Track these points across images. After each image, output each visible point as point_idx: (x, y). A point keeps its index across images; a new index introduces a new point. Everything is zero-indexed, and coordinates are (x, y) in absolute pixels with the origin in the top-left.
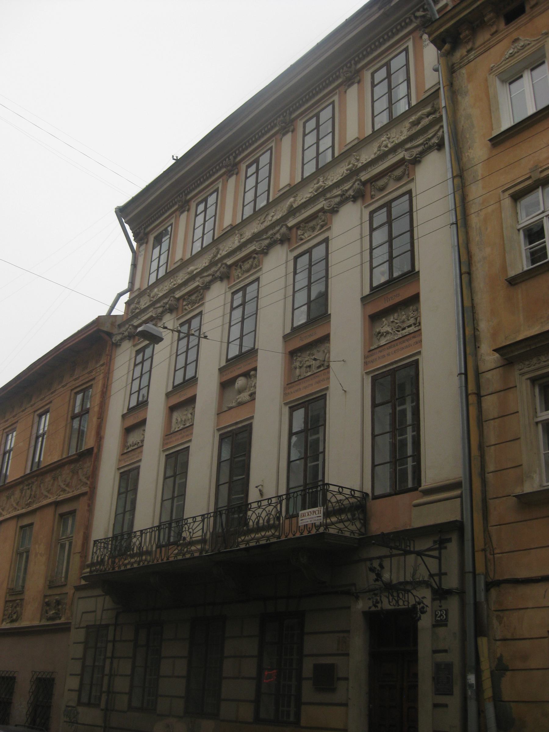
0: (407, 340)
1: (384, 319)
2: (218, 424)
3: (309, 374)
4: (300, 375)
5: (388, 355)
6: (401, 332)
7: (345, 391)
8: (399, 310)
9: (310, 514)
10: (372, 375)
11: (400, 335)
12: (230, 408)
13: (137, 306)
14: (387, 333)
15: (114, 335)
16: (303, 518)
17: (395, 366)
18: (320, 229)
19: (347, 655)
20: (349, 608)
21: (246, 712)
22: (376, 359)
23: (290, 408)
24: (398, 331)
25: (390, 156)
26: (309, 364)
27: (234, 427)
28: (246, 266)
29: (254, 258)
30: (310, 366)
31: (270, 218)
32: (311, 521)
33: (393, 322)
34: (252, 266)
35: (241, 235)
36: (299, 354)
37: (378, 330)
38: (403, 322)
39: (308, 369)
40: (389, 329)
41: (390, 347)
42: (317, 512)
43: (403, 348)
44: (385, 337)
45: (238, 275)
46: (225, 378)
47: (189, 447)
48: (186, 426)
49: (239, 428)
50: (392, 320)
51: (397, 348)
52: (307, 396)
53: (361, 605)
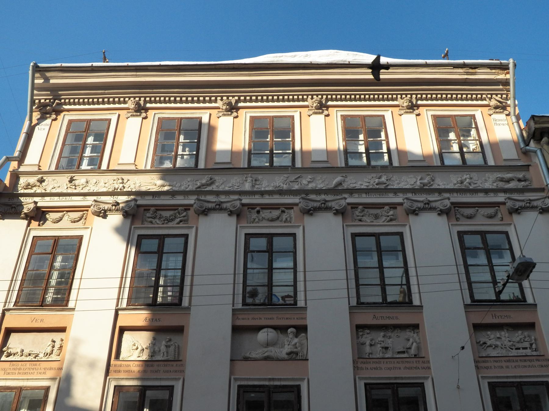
0: (530, 361)
1: (489, 333)
2: (232, 373)
3: (387, 356)
4: (371, 354)
7: (458, 387)
8: (505, 330)
11: (514, 353)
12: (246, 359)
14: (496, 346)
17: (519, 380)
18: (388, 222)
23: (366, 384)
24: (512, 349)
26: (386, 346)
27: (267, 383)
28: (266, 214)
29: (283, 212)
30: (386, 348)
31: (305, 182)
33: (498, 338)
34: (278, 218)
35: (256, 180)
36: (368, 331)
37: (483, 340)
38: (518, 342)
39: (384, 350)
40: (498, 343)
41: (509, 361)
43: (525, 366)
44: (494, 349)
45: (255, 219)
46: (239, 323)
47: (173, 387)
49: (276, 386)
50: (498, 336)
52: (396, 378)
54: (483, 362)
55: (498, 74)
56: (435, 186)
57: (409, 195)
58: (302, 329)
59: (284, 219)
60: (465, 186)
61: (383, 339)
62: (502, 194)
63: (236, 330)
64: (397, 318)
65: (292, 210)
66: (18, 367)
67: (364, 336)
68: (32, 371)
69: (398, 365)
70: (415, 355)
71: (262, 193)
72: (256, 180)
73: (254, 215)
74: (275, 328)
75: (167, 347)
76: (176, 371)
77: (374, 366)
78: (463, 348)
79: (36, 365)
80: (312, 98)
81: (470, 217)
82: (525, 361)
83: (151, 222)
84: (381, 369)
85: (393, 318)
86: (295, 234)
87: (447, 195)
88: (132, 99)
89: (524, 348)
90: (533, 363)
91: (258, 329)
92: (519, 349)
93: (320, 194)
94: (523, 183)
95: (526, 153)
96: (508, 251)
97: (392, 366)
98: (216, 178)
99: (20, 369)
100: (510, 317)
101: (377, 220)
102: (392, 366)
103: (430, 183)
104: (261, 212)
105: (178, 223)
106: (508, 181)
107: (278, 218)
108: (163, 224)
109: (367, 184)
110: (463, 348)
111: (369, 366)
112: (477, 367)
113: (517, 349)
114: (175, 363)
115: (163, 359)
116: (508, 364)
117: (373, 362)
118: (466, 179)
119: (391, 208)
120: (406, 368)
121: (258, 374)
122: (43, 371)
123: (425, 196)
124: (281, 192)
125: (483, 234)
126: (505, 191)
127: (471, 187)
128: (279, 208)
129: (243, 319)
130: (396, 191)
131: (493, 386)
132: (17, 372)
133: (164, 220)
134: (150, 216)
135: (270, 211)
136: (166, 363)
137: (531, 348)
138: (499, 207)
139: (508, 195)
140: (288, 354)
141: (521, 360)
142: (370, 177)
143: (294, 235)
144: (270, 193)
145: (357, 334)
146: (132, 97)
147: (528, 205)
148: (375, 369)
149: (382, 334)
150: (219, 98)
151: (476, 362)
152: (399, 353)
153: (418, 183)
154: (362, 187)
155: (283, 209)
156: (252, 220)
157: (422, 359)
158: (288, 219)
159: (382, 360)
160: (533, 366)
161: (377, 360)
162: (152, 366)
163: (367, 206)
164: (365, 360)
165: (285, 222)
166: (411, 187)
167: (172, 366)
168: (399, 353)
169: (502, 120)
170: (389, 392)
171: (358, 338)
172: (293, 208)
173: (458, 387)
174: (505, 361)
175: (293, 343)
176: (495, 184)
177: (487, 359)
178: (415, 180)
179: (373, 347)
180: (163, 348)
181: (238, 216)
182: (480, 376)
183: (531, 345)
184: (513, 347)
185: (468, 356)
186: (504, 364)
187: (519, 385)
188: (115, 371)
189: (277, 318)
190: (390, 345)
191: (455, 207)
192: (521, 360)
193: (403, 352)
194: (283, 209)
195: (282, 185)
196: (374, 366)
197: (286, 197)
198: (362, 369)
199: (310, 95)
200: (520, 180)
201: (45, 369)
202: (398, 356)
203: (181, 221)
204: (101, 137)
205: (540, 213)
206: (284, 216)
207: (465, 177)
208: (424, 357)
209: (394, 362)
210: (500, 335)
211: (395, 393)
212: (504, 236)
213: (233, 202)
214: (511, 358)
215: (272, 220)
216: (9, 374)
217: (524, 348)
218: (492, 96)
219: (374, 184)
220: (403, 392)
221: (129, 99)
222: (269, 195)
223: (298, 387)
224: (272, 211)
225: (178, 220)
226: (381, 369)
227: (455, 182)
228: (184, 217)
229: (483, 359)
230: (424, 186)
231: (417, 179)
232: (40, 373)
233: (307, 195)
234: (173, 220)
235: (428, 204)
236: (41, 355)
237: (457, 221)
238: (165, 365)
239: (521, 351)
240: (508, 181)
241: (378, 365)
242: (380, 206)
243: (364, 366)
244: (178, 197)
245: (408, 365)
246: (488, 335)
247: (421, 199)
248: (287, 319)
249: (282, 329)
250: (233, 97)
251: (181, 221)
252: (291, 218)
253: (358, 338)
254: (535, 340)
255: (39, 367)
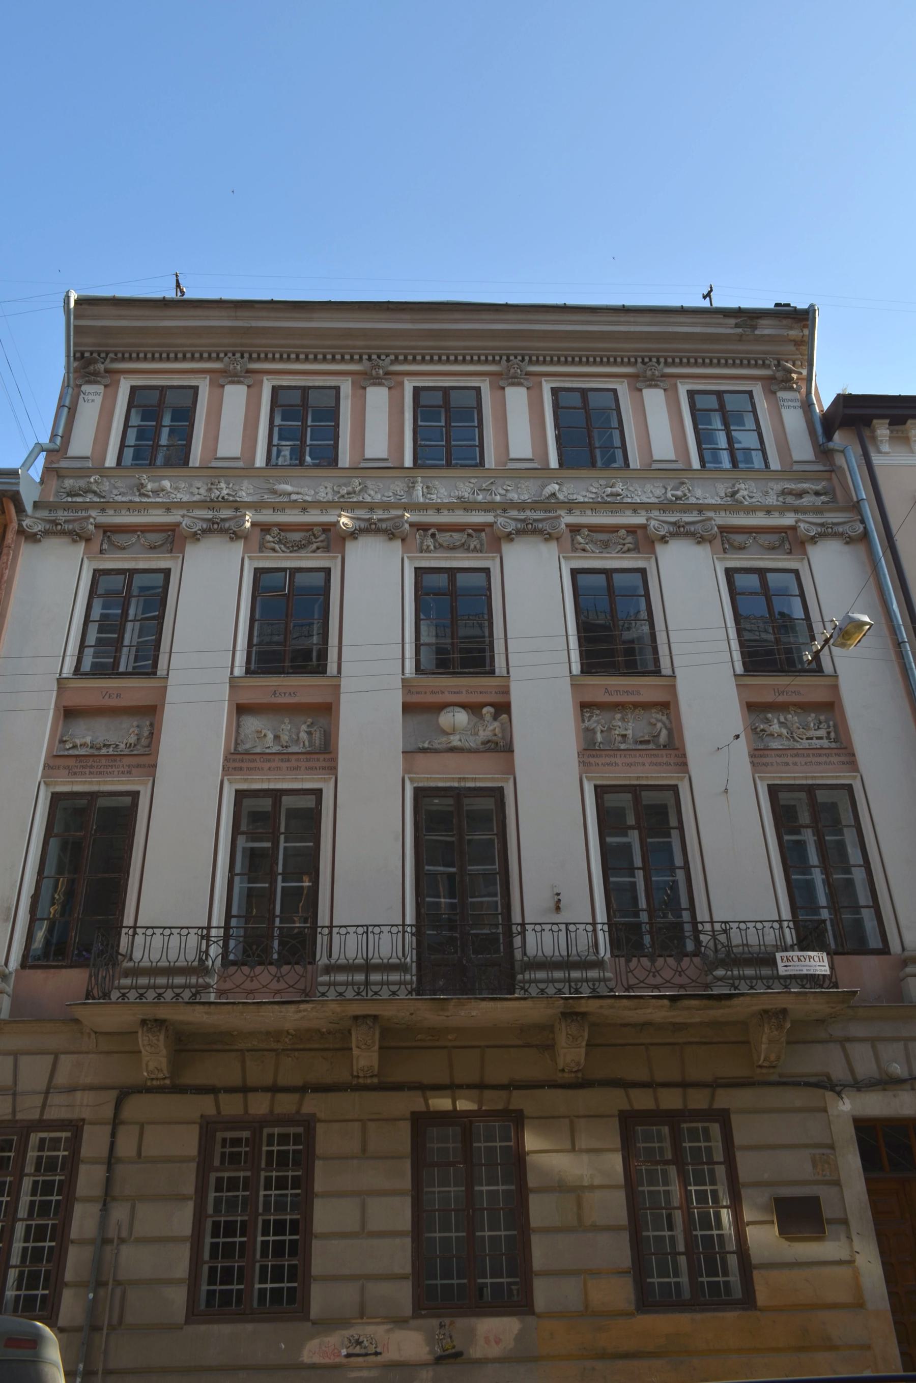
0: (827, 755)
1: (770, 715)
5: (795, 764)
6: (804, 741)
7: (726, 791)
9: (802, 958)
10: (770, 782)
12: (424, 750)
13: (94, 487)
14: (780, 735)
15: (27, 516)
16: (788, 964)
18: (624, 552)
19: (837, 1183)
20: (825, 1110)
21: (618, 1292)
22: (772, 764)
25: (760, 514)
26: (624, 733)
27: (456, 784)
28: (443, 538)
32: (808, 970)
36: (598, 712)
41: (797, 755)
42: (816, 959)
43: (820, 763)
45: (428, 547)
48: (290, 750)
49: (469, 788)
50: (782, 719)
51: (809, 759)
53: (846, 1107)
54: (761, 756)
55: (791, 328)
56: (693, 500)
57: (655, 513)
58: (503, 708)
59: (472, 547)
60: (737, 501)
61: (620, 724)
62: (792, 515)
63: (408, 708)
64: (639, 693)
65: (483, 534)
66: (89, 764)
67: (595, 718)
68: (110, 770)
69: (641, 760)
70: (665, 746)
71: (438, 509)
72: (428, 487)
73: (429, 542)
74: (463, 706)
75: (309, 733)
76: (324, 768)
77: (608, 760)
78: (737, 737)
79: (115, 761)
80: (508, 360)
81: (741, 548)
82: (820, 755)
83: (274, 550)
84: (617, 764)
85: (633, 693)
86: (489, 569)
87: (710, 514)
88: (230, 355)
89: (818, 738)
90: (832, 759)
91: (442, 707)
92: (811, 739)
93: (524, 510)
94: (822, 497)
95: (824, 453)
96: (799, 598)
97: (632, 760)
98: (369, 483)
99: (91, 767)
100: (799, 693)
101: (609, 550)
102: (632, 760)
103: (685, 495)
104: (437, 536)
105: (314, 552)
106: (800, 495)
107: (463, 544)
108: (291, 552)
109: (593, 496)
110: (737, 737)
111: (600, 761)
112: (753, 763)
113: (807, 739)
114: (321, 757)
115: (304, 750)
116: (796, 759)
117: (606, 756)
118: (737, 492)
119: (628, 532)
120: (652, 764)
121: (444, 773)
122: (126, 769)
123: (678, 514)
124: (467, 506)
125: (762, 573)
126: (796, 510)
127: (746, 503)
128: (463, 530)
129: (418, 693)
130: (635, 508)
131: (774, 791)
132: (87, 771)
133: (292, 546)
134: (271, 539)
135: (449, 534)
136: (308, 756)
137: (828, 738)
138: (786, 533)
139: (800, 516)
140: (483, 743)
141: (814, 755)
142: (596, 485)
143: (487, 571)
144: (450, 507)
145: (582, 716)
146: (230, 351)
147: (830, 530)
148: (608, 764)
149: (618, 716)
150: (365, 357)
151: (752, 756)
152: (641, 742)
153: (669, 495)
154: (586, 500)
155: (470, 531)
156: (425, 547)
157: (676, 752)
158: (478, 546)
159: (619, 753)
160: (830, 763)
161: (612, 753)
162: (288, 760)
163: (593, 529)
164: (594, 753)
165: (473, 551)
166: (656, 501)
167: (318, 760)
168: (641, 742)
169: (792, 401)
170: (629, 796)
171: (583, 721)
172: (483, 530)
173: (726, 791)
174: (791, 756)
175: (491, 728)
176: (781, 499)
177: (766, 752)
178: (663, 491)
179: (605, 734)
180: (303, 736)
181: (403, 540)
182: (757, 775)
183: (829, 733)
184: (804, 737)
185: (742, 748)
186: (790, 760)
187: (810, 790)
188: (235, 769)
189: (467, 691)
190: (629, 732)
191: (721, 532)
192: (814, 755)
193: (648, 742)
194: (470, 531)
195: (466, 495)
196: (608, 760)
197: (474, 513)
198: (590, 764)
199: (505, 354)
200: (817, 494)
201: (129, 766)
202: (640, 747)
203: (318, 548)
204: (186, 415)
205: (847, 543)
206: (474, 543)
207: (737, 486)
208: (677, 749)
209: (635, 756)
210: (786, 719)
211: (637, 799)
212: (793, 575)
213: (396, 520)
214: (800, 752)
215: (453, 548)
216: (75, 773)
217: (818, 738)
218: (779, 362)
219: (604, 495)
220: (648, 798)
221: (226, 355)
222: (449, 510)
223: (501, 790)
224: (453, 534)
225: (314, 546)
226: (617, 764)
227: (723, 495)
228: (322, 541)
229: (761, 752)
230: (677, 499)
231: (666, 489)
232: (123, 773)
233: (505, 510)
234: (305, 546)
235: (683, 527)
236: (122, 746)
237: (725, 552)
238: (308, 760)
239: (814, 741)
240: (800, 495)
241: (613, 760)
242: (614, 529)
243: (592, 760)
244: (313, 512)
245: (654, 760)
246: (767, 719)
247: (673, 520)
248: (481, 693)
249: (474, 709)
250: (387, 356)
251: (318, 548)
252: (482, 545)
253: (583, 721)
254: (835, 726)
255: (121, 764)
